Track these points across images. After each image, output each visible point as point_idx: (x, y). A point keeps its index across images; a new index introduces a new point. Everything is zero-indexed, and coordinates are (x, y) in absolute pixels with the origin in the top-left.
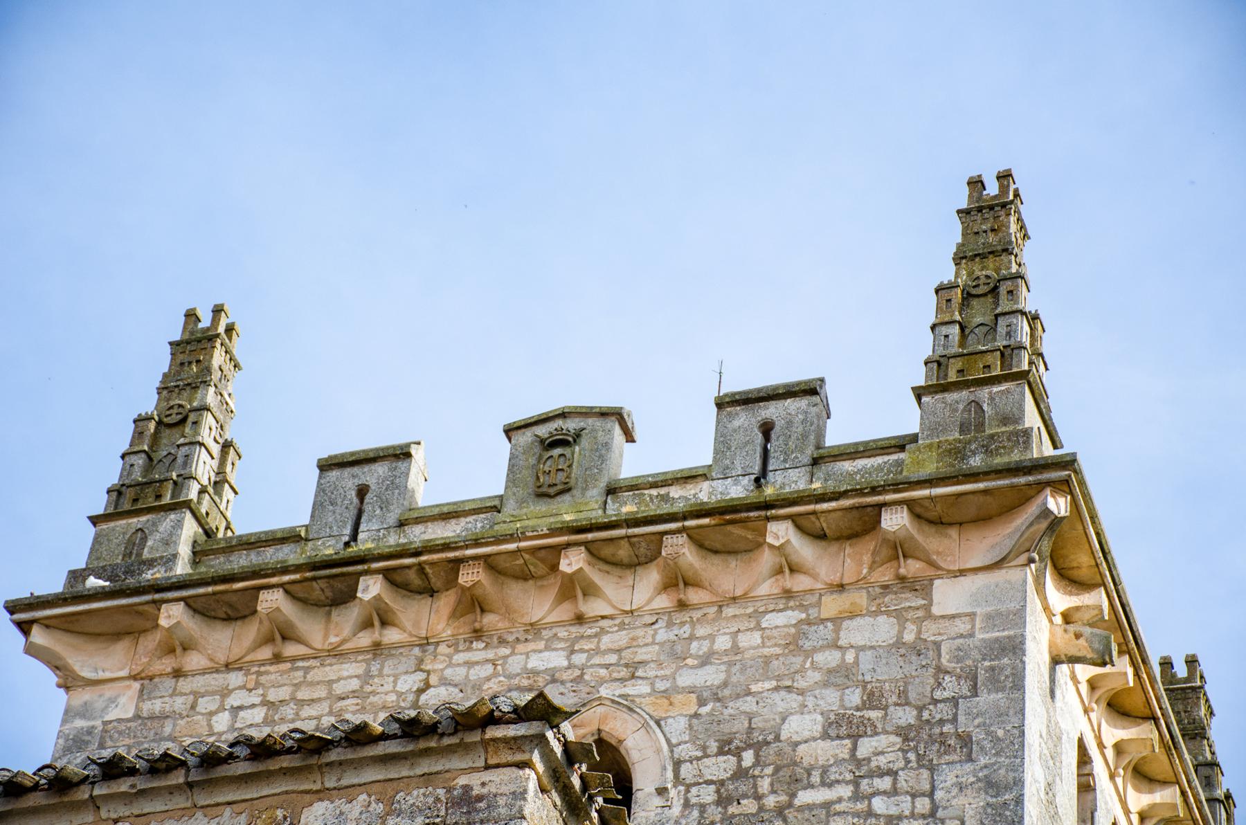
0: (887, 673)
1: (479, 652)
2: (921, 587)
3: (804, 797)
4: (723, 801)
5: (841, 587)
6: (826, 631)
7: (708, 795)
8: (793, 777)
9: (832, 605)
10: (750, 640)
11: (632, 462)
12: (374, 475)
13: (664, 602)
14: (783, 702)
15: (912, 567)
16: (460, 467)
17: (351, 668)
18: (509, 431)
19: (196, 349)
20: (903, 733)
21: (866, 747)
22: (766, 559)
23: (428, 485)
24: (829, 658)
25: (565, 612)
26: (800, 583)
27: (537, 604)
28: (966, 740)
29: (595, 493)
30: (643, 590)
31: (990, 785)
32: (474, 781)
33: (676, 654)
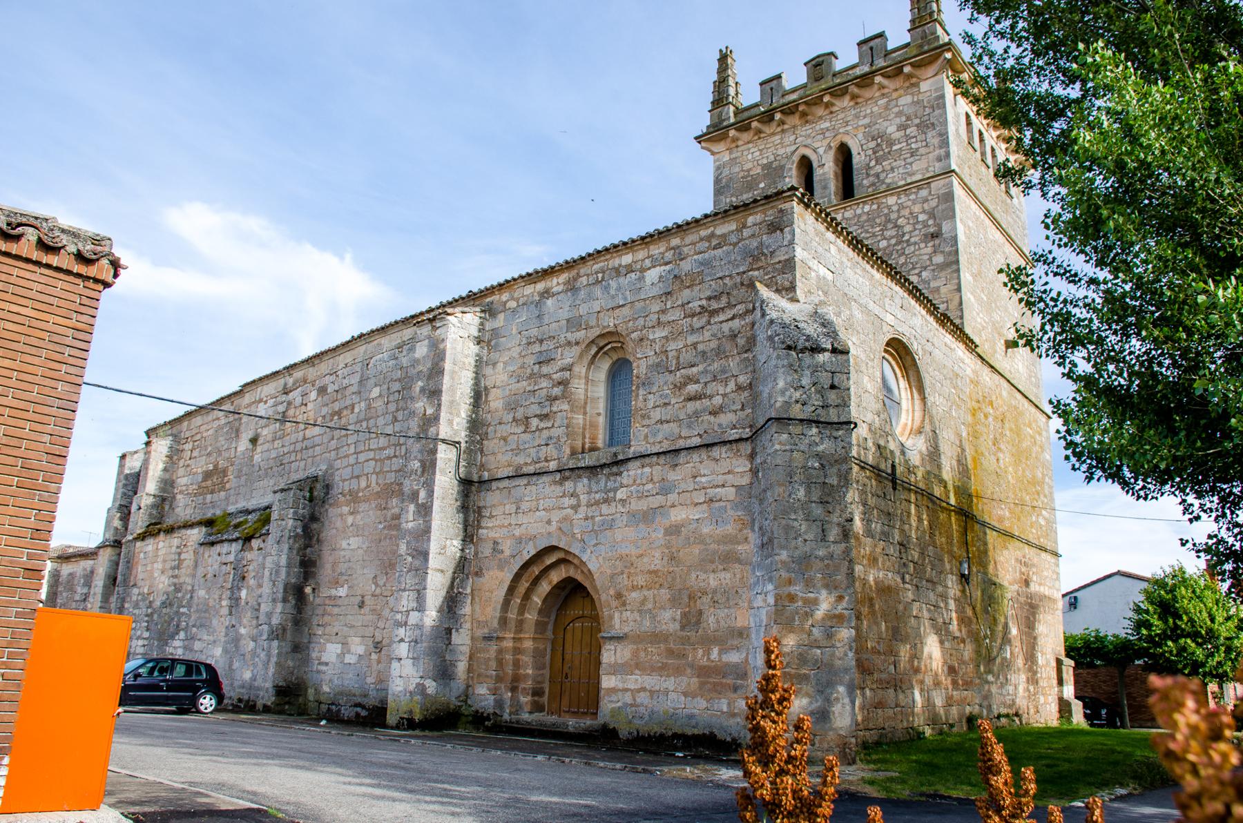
0: (909, 111)
2: (916, 85)
3: (895, 148)
4: (874, 153)
5: (896, 90)
6: (894, 103)
7: (870, 152)
8: (891, 143)
9: (895, 95)
11: (839, 65)
12: (774, 84)
13: (852, 103)
14: (886, 124)
15: (914, 80)
16: (795, 77)
17: (777, 137)
18: (805, 64)
20: (917, 126)
21: (908, 131)
22: (876, 87)
23: (788, 84)
24: (896, 110)
25: (827, 112)
26: (886, 91)
27: (820, 111)
28: (933, 124)
29: (830, 77)
30: (846, 102)
31: (941, 135)
32: (782, 206)
33: (857, 117)
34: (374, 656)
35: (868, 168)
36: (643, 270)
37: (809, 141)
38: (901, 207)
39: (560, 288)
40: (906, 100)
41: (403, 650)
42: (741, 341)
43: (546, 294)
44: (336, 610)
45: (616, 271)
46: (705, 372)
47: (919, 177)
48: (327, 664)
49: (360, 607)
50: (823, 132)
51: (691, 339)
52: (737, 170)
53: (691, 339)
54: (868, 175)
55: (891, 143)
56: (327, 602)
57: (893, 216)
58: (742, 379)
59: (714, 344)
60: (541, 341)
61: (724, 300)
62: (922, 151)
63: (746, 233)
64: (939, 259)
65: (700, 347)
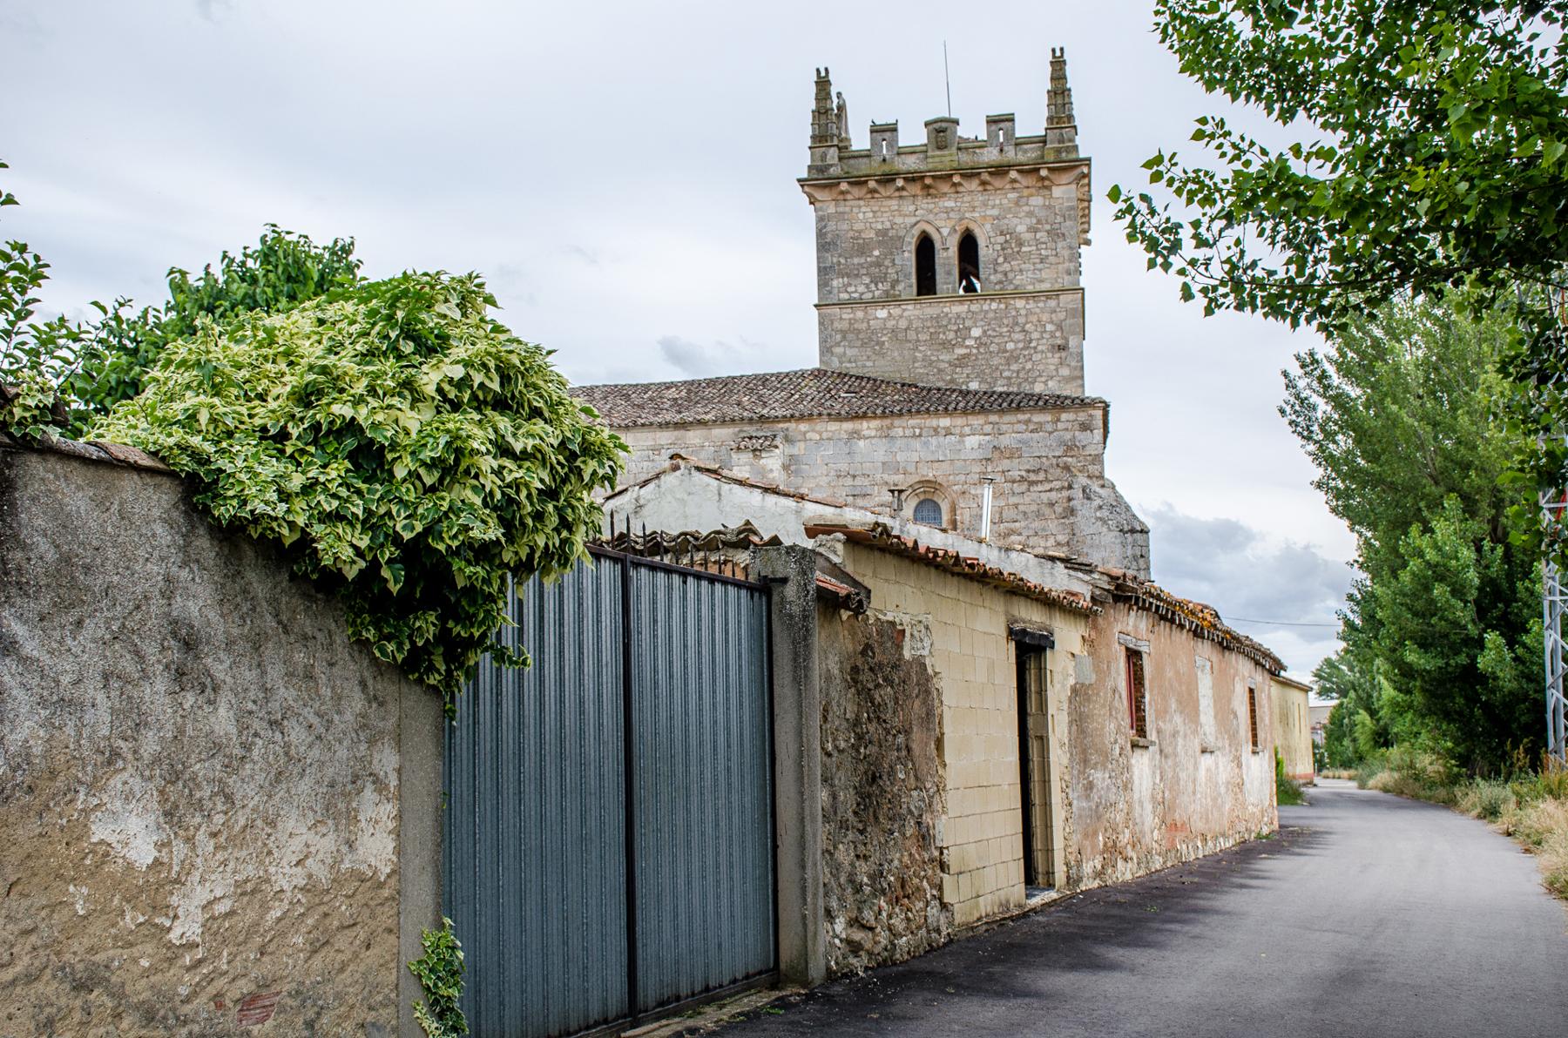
0: (1042, 214)
1: (929, 200)
2: (1048, 188)
9: (1026, 192)
10: (1005, 201)
12: (887, 135)
14: (1016, 221)
15: (1047, 183)
16: (913, 135)
18: (927, 124)
19: (823, 84)
24: (1026, 208)
27: (945, 188)
29: (954, 149)
30: (974, 185)
35: (996, 263)
36: (962, 435)
37: (931, 217)
38: (1030, 312)
39: (873, 433)
40: (1037, 201)
42: (1059, 509)
43: (856, 435)
45: (936, 430)
46: (1027, 527)
47: (1046, 286)
50: (947, 211)
51: (1013, 500)
52: (845, 227)
53: (1013, 500)
54: (996, 271)
55: (1021, 245)
57: (1021, 320)
58: (1062, 538)
59: (1034, 507)
60: (854, 477)
61: (1041, 476)
62: (1052, 259)
63: (1060, 426)
64: (1065, 372)
65: (1021, 508)
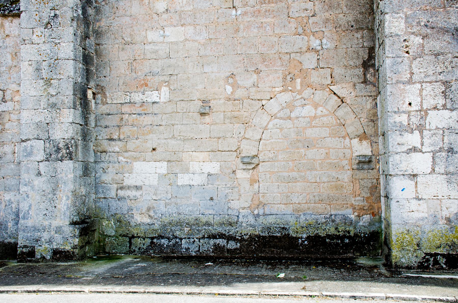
34: (241, 174)
41: (421, 163)
44: (147, 120)
48: (137, 188)
49: (203, 114)
56: (126, 109)
